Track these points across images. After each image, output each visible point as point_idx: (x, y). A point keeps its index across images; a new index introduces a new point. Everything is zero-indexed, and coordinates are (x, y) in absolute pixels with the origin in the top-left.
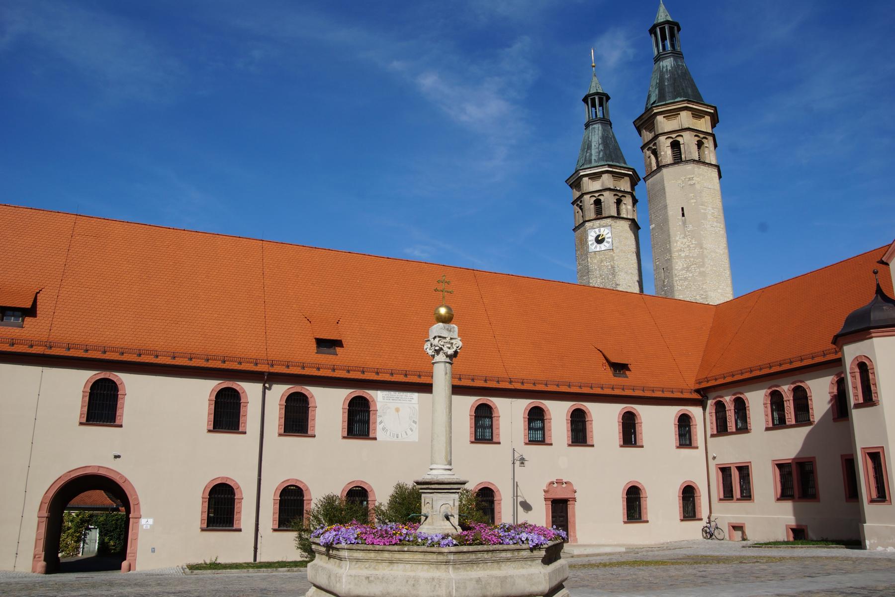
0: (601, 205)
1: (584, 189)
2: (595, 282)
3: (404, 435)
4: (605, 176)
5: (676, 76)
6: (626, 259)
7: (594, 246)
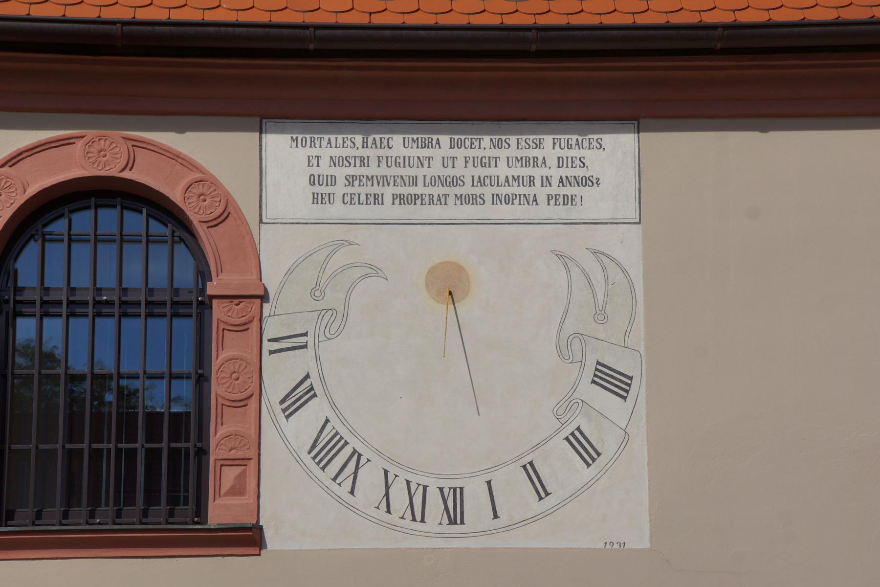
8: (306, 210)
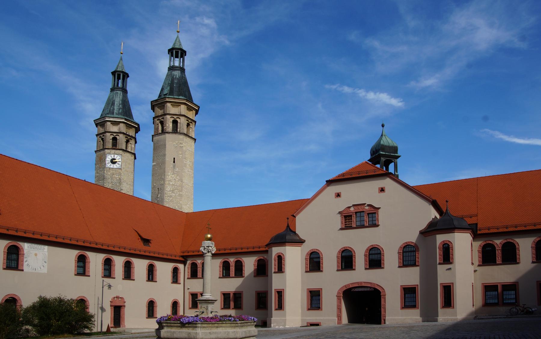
0: (117, 141)
1: (107, 129)
2: (108, 185)
3: (39, 269)
4: (122, 125)
5: (181, 83)
6: (128, 176)
7: (110, 164)
8: (28, 249)
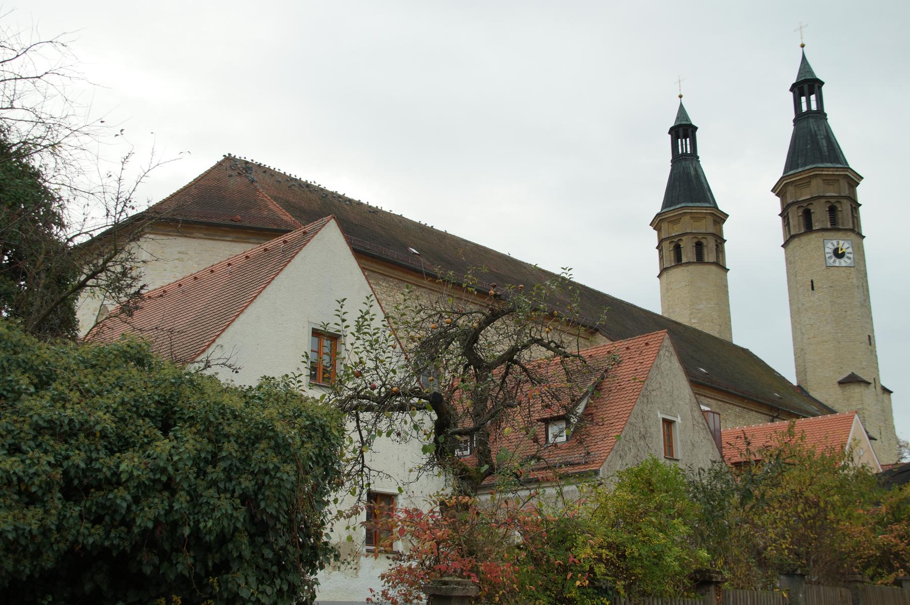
7: (830, 255)
